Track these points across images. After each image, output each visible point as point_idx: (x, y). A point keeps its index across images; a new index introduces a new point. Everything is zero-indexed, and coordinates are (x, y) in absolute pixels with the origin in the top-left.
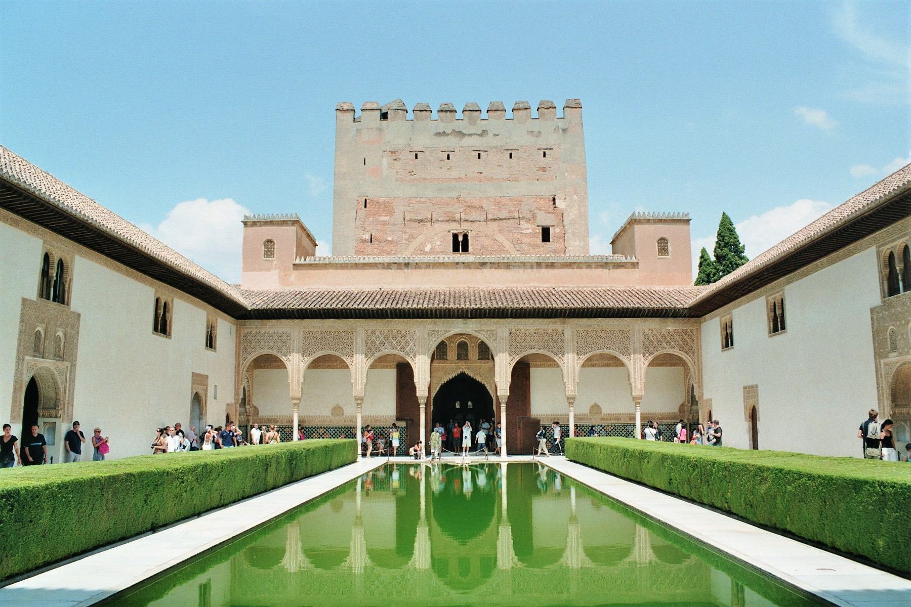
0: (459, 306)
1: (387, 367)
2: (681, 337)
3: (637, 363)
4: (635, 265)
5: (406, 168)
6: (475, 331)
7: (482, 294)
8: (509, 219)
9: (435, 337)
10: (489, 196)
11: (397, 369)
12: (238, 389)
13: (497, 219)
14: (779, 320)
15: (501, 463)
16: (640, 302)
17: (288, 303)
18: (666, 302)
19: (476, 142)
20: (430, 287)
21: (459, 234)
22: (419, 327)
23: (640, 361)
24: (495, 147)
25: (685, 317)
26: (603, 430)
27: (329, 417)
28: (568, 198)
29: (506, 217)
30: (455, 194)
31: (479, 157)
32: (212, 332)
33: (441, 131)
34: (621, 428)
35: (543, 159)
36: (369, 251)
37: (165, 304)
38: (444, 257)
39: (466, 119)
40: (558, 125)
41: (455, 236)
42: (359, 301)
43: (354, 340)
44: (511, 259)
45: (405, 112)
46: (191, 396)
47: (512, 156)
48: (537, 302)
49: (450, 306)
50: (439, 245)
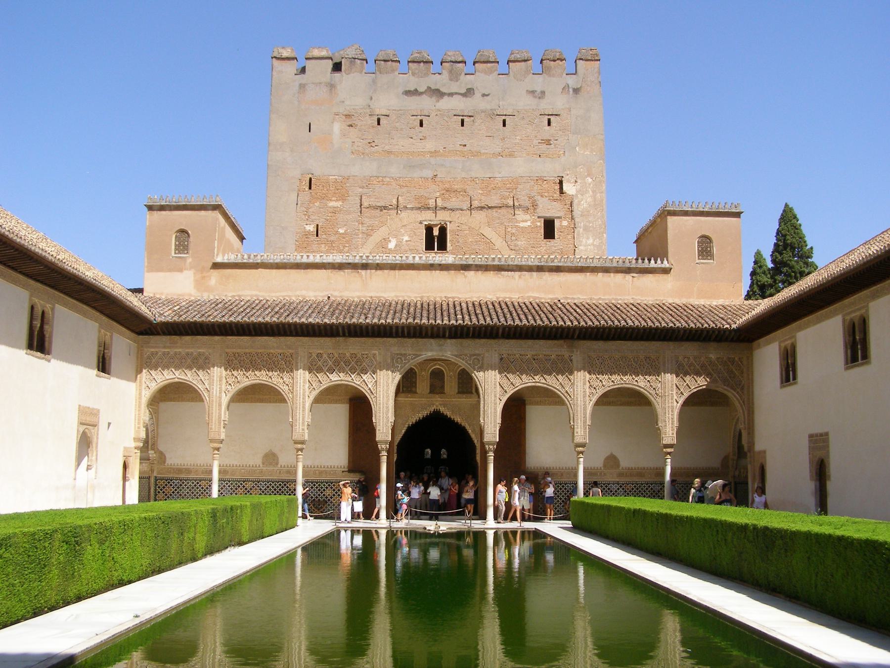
0: (434, 322)
1: (336, 402)
2: (726, 367)
3: (668, 401)
4: (666, 271)
5: (362, 138)
6: (454, 355)
7: (464, 305)
8: (500, 207)
9: (401, 363)
10: (474, 175)
11: (350, 404)
12: (139, 428)
13: (484, 208)
14: (859, 347)
17: (206, 315)
18: (707, 320)
19: (457, 104)
20: (397, 297)
22: (380, 349)
23: (672, 399)
24: (483, 111)
25: (732, 340)
26: (621, 489)
27: (259, 466)
28: (579, 181)
29: (496, 205)
30: (429, 173)
31: (462, 125)
32: (105, 351)
33: (412, 89)
34: (644, 487)
35: (549, 127)
36: (315, 247)
37: (43, 313)
38: (414, 257)
39: (445, 74)
40: (568, 83)
41: (429, 229)
42: (301, 313)
43: (294, 364)
44: (503, 260)
45: (365, 62)
46: (77, 437)
48: (537, 318)
49: (423, 322)
50: (407, 241)
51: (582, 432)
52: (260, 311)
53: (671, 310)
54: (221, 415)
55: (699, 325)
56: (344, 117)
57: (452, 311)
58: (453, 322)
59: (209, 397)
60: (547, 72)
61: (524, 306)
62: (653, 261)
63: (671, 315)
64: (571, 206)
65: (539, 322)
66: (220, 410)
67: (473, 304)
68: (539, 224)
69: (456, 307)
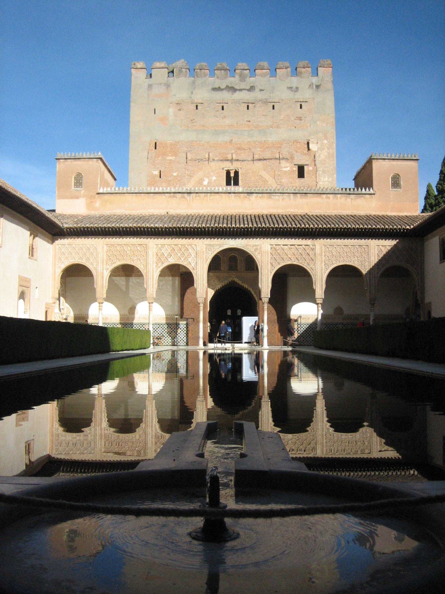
1: (173, 276)
7: (249, 217)
8: (271, 159)
12: (54, 291)
15: (262, 350)
16: (376, 224)
17: (94, 223)
18: (396, 224)
21: (231, 171)
24: (260, 100)
28: (319, 143)
29: (269, 158)
30: (227, 138)
31: (248, 109)
33: (217, 87)
35: (300, 110)
38: (219, 189)
39: (237, 77)
41: (228, 173)
44: (272, 189)
45: (188, 70)
46: (18, 293)
47: (275, 107)
48: (293, 223)
50: (214, 180)
51: (320, 292)
52: (126, 221)
53: (375, 219)
54: (103, 283)
55: (391, 227)
56: (176, 105)
57: (241, 220)
58: (242, 226)
59: (96, 273)
60: (300, 76)
61: (285, 217)
62: (363, 190)
63: (374, 221)
64: (315, 158)
65: (294, 226)
66: (103, 280)
67: (255, 216)
68: (295, 169)
69: (243, 218)
